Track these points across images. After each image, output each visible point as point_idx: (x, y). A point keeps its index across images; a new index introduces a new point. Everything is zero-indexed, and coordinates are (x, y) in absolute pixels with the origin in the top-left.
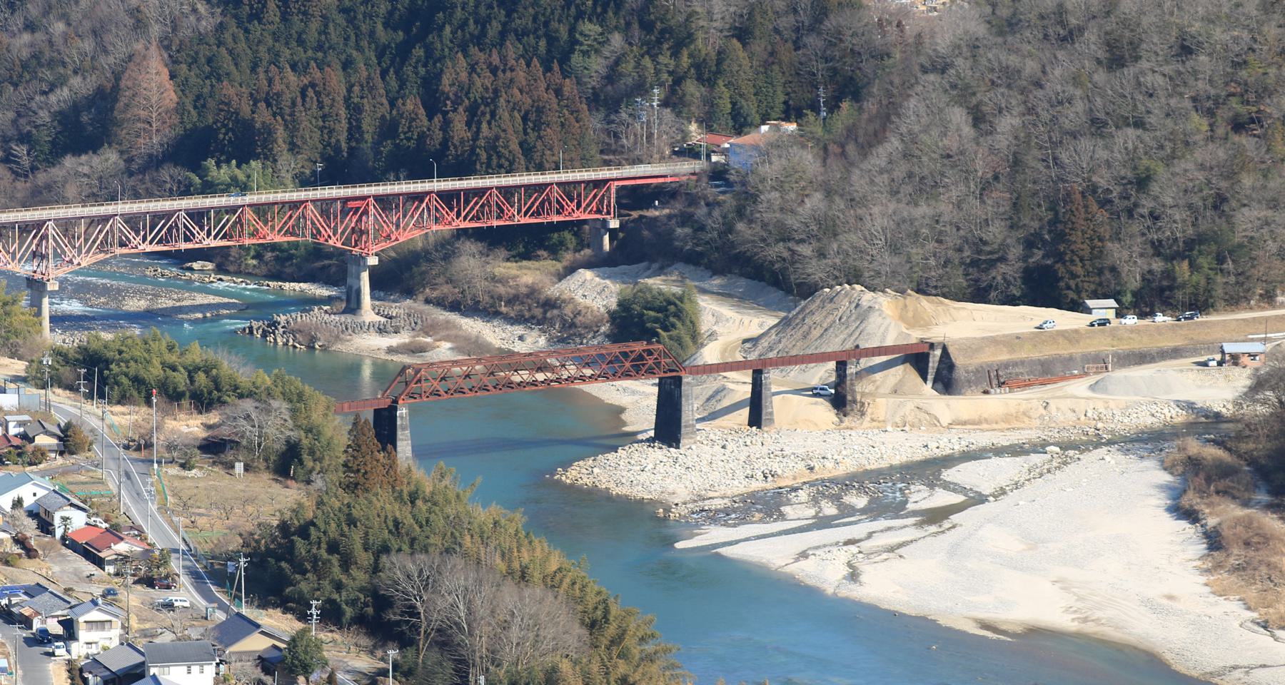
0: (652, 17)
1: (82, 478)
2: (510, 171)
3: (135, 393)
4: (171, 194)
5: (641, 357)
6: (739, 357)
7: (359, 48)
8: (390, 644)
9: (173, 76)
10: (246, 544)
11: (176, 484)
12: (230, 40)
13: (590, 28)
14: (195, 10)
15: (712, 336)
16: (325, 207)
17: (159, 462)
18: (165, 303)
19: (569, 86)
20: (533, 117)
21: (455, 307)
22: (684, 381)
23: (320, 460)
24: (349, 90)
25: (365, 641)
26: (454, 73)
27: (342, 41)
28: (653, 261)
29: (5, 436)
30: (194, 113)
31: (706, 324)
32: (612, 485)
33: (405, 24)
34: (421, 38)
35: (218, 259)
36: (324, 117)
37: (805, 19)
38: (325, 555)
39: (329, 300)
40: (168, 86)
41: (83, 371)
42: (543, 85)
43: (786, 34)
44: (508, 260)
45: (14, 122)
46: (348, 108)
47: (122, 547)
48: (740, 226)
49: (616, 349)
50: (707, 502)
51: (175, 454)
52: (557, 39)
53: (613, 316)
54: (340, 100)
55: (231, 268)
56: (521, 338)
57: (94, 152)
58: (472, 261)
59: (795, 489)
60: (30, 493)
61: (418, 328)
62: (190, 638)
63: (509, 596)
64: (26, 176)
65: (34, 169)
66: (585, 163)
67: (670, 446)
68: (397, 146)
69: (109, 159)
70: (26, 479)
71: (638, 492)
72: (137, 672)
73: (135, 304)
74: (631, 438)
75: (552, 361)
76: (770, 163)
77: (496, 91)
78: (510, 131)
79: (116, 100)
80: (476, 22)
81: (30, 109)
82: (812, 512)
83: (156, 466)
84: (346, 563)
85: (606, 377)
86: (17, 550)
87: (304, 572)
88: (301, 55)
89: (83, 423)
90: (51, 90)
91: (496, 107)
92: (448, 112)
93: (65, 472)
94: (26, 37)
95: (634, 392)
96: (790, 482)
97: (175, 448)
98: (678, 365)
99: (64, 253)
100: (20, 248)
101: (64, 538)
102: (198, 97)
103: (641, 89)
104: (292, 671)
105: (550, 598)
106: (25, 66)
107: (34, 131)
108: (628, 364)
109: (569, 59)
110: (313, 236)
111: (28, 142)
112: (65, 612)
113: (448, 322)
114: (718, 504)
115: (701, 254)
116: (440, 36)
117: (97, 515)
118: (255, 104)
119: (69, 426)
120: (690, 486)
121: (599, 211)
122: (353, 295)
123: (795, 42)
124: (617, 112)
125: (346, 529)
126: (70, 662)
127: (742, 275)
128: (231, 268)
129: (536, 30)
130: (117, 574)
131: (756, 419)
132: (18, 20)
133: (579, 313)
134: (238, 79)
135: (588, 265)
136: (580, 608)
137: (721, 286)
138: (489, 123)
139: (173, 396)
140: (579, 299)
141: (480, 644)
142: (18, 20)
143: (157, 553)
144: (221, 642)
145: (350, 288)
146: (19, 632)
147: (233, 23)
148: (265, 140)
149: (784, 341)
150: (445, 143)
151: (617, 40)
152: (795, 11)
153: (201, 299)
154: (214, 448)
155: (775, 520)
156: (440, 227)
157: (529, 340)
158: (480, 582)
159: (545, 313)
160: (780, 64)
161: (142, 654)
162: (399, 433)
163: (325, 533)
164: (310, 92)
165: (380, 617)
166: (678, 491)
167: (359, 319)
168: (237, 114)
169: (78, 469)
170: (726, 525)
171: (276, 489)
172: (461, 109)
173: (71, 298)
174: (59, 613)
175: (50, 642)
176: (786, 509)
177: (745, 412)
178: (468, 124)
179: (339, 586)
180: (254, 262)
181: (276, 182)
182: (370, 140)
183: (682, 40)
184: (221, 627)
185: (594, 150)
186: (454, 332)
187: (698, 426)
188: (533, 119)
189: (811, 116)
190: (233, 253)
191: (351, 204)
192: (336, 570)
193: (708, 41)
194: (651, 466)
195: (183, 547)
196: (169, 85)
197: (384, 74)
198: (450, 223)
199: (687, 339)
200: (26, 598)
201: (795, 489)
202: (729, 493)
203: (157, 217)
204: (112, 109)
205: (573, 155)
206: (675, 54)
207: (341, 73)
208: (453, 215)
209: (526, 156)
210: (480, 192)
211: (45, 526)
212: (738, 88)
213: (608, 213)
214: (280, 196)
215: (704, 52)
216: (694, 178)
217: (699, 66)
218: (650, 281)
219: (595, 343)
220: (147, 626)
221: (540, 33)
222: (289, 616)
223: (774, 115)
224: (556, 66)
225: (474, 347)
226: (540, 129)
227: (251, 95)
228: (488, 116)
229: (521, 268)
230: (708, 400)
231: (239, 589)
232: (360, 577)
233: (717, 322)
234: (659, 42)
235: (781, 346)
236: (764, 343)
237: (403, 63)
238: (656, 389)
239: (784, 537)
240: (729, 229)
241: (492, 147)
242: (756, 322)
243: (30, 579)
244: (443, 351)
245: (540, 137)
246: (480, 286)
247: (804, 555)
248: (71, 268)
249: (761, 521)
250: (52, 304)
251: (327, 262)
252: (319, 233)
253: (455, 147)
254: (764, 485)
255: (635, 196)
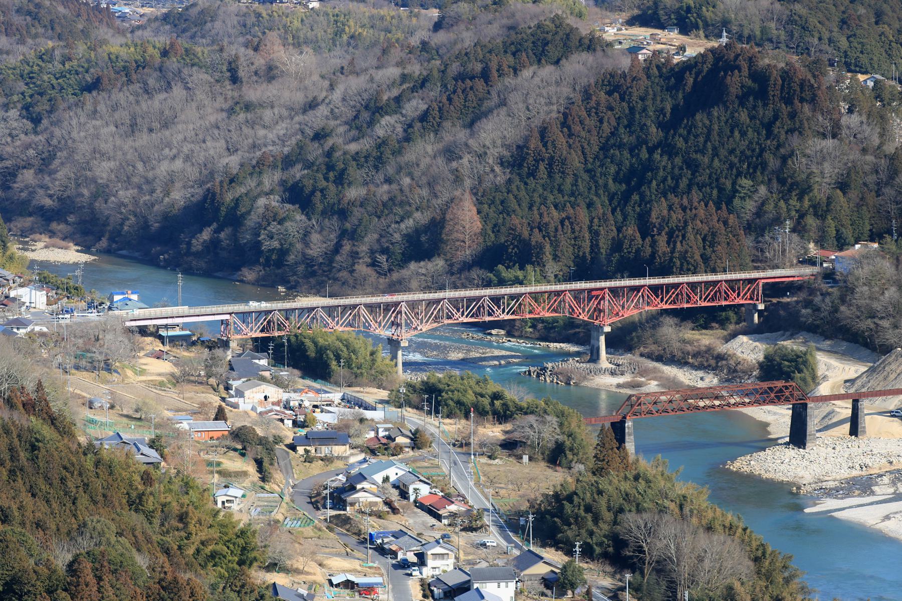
0: (785, 175)
1: (426, 464)
2: (695, 273)
3: (458, 411)
4: (477, 287)
5: (781, 391)
6: (843, 392)
7: (597, 195)
8: (626, 571)
9: (479, 212)
10: (532, 506)
11: (485, 468)
12: (515, 189)
13: (746, 182)
14: (493, 171)
15: (825, 378)
16: (577, 294)
17: (475, 455)
18: (474, 355)
19: (732, 219)
20: (709, 238)
21: (659, 359)
22: (809, 406)
23: (577, 454)
24: (591, 221)
25: (609, 569)
26: (659, 211)
27: (586, 190)
28: (786, 330)
29: (377, 437)
30: (492, 235)
31: (821, 371)
32: (763, 472)
33: (627, 180)
34: (638, 188)
35: (508, 328)
36: (575, 238)
37: (883, 176)
38: (583, 514)
39: (578, 354)
40: (476, 218)
41: (426, 396)
42: (716, 219)
43: (872, 186)
44: (693, 329)
45: (378, 241)
46: (590, 232)
47: (453, 508)
48: (843, 308)
49: (765, 385)
50: (824, 483)
51: (485, 450)
52: (724, 189)
53: (761, 365)
54: (585, 228)
55: (516, 334)
56: (702, 379)
57: (429, 260)
58: (671, 330)
59: (881, 476)
60: (395, 472)
61: (636, 371)
62: (498, 565)
63: (703, 540)
64: (386, 275)
65: (390, 270)
66: (743, 268)
67: (800, 448)
68: (621, 257)
69: (439, 263)
70: (391, 464)
71: (779, 477)
72: (464, 588)
73: (455, 356)
74: (774, 442)
75: (724, 393)
76: (862, 268)
77: (686, 222)
78: (695, 247)
79: (443, 227)
80: (672, 179)
81: (388, 233)
82: (892, 490)
83: (473, 457)
84: (596, 519)
85: (758, 403)
86: (386, 509)
87: (569, 525)
88: (560, 199)
89: (426, 429)
90: (402, 221)
91: (686, 232)
92: (654, 236)
93: (415, 460)
94: (386, 187)
95: (775, 414)
96: (877, 472)
97: (485, 445)
98: (804, 396)
99: (412, 322)
100: (384, 317)
101: (415, 502)
102: (495, 225)
103: (778, 221)
104: (563, 587)
105: (729, 542)
106: (384, 205)
107: (391, 246)
108: (773, 395)
109: (732, 202)
110: (570, 314)
111: (387, 254)
112: (419, 548)
113: (655, 368)
114: (831, 484)
115: (817, 326)
116: (649, 187)
117: (436, 487)
118: (531, 230)
119: (417, 431)
120: (813, 473)
121: (751, 299)
122: (595, 351)
123: (876, 192)
124: (763, 236)
125: (596, 497)
126: (422, 580)
127: (843, 339)
128: (516, 334)
129: (711, 184)
130: (450, 525)
131: (854, 431)
132: (380, 177)
133: (739, 363)
134: (520, 214)
135: (745, 333)
136: (748, 548)
137: (830, 345)
138: (681, 242)
139: (482, 413)
140: (739, 354)
141: (684, 570)
142: (380, 177)
143: (475, 512)
144: (518, 568)
145: (593, 346)
146: (390, 560)
147: (517, 178)
148: (538, 253)
149: (872, 381)
150: (653, 255)
151: (763, 190)
152: (877, 172)
153: (497, 353)
154: (510, 446)
155: (868, 495)
156: (651, 308)
157: (707, 380)
158: (682, 531)
159: (717, 363)
160: (867, 205)
161: (469, 575)
162: (627, 437)
163: (583, 500)
164: (567, 223)
165: (620, 554)
166: (805, 476)
167: (599, 366)
168: (520, 236)
169: (423, 459)
170: (836, 498)
171: (549, 472)
172: (663, 233)
173: (414, 352)
174: (415, 548)
175: (409, 567)
176: (875, 488)
177: (847, 427)
178: (668, 243)
179: (591, 534)
180: (531, 330)
181: (544, 279)
182: (604, 253)
183: (804, 190)
184: (517, 558)
185: (748, 260)
186: (659, 375)
187: (818, 435)
188: (709, 239)
189: (888, 238)
190: (517, 324)
191: (594, 293)
192: (590, 524)
193: (821, 190)
194: (787, 460)
195: (491, 508)
196: (476, 217)
197: (613, 211)
198: (656, 306)
199: (809, 380)
200: (393, 539)
201: (881, 476)
202: (838, 478)
203: (470, 300)
204: (440, 234)
205: (735, 263)
206: (800, 198)
207: (586, 210)
208: (659, 300)
209: (704, 263)
210: (676, 286)
211: (404, 495)
212: (840, 221)
213: (757, 300)
214: (549, 288)
215: (818, 198)
216: (813, 278)
217: (815, 206)
218: (785, 343)
219: (750, 383)
220: (470, 558)
221: (714, 185)
222: (560, 553)
223: (863, 238)
224: (724, 206)
225: (672, 385)
226: (714, 246)
227: (529, 224)
228: (680, 238)
229: (701, 334)
230: (823, 418)
231: (528, 535)
232: (605, 527)
233: (828, 370)
234: (790, 191)
235: (869, 385)
236: (859, 383)
237: (625, 205)
238: (790, 412)
239: (874, 506)
240: (836, 310)
241: (684, 257)
242: (853, 370)
243: (396, 528)
244: (653, 386)
245: (714, 251)
246: (676, 345)
247: (887, 517)
248: (416, 333)
249: (859, 495)
250: (403, 355)
251: (577, 330)
252: (573, 310)
253: (660, 258)
254: (860, 473)
255: (774, 289)
